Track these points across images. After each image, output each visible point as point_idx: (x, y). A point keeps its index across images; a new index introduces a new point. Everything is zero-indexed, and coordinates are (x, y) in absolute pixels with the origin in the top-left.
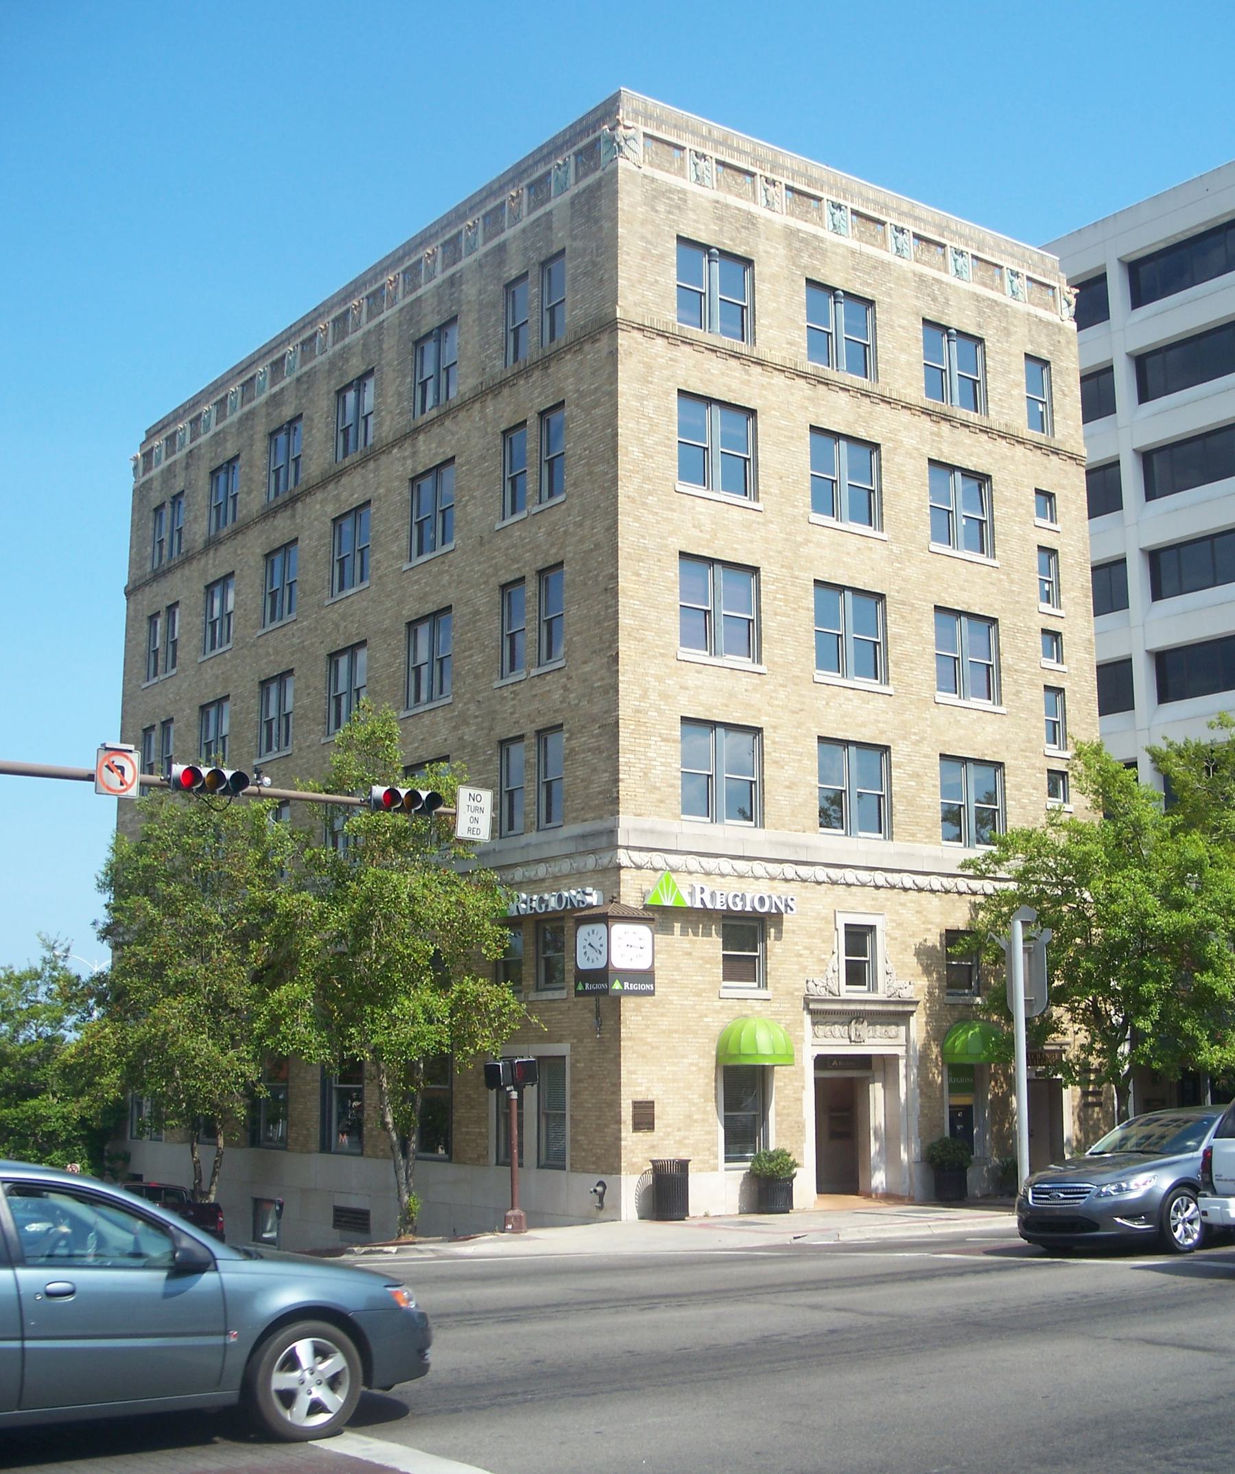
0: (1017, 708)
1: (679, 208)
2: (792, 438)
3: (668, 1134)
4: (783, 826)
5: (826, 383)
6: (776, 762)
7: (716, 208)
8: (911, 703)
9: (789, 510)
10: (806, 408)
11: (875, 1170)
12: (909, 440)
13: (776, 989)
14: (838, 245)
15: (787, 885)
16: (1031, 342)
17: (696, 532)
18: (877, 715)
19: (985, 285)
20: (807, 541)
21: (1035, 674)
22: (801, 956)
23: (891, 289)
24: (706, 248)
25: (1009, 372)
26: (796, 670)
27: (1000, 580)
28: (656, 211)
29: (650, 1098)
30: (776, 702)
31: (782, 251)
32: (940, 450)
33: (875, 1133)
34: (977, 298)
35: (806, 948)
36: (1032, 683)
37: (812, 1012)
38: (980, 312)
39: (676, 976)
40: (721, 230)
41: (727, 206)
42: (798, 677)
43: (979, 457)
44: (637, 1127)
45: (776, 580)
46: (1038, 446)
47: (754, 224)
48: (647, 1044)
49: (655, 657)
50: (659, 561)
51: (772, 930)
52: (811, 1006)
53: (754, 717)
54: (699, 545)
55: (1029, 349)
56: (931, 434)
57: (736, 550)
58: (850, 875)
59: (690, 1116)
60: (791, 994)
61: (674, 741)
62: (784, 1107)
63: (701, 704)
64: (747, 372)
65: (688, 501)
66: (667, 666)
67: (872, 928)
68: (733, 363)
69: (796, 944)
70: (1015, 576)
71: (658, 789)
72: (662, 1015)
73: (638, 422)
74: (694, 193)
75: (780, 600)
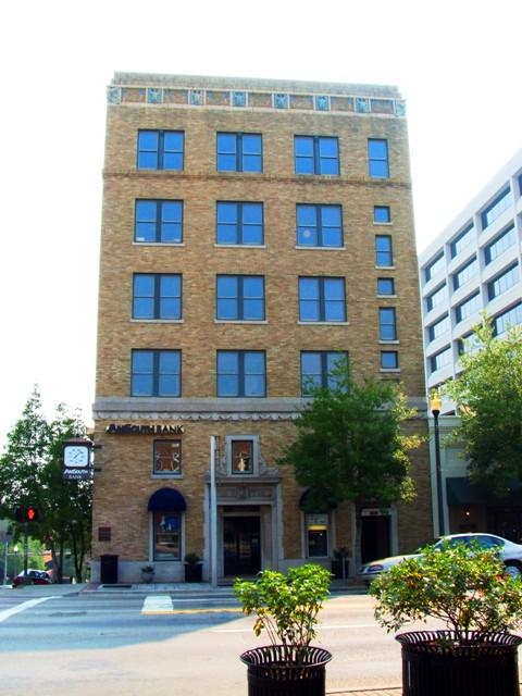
4: (193, 395)
5: (228, 179)
9: (201, 244)
16: (373, 131)
17: (143, 263)
20: (213, 257)
26: (203, 319)
38: (335, 124)
39: (125, 469)
44: (100, 539)
55: (371, 136)
58: (235, 417)
59: (132, 535)
63: (143, 341)
67: (252, 441)
70: (358, 253)
71: (116, 383)
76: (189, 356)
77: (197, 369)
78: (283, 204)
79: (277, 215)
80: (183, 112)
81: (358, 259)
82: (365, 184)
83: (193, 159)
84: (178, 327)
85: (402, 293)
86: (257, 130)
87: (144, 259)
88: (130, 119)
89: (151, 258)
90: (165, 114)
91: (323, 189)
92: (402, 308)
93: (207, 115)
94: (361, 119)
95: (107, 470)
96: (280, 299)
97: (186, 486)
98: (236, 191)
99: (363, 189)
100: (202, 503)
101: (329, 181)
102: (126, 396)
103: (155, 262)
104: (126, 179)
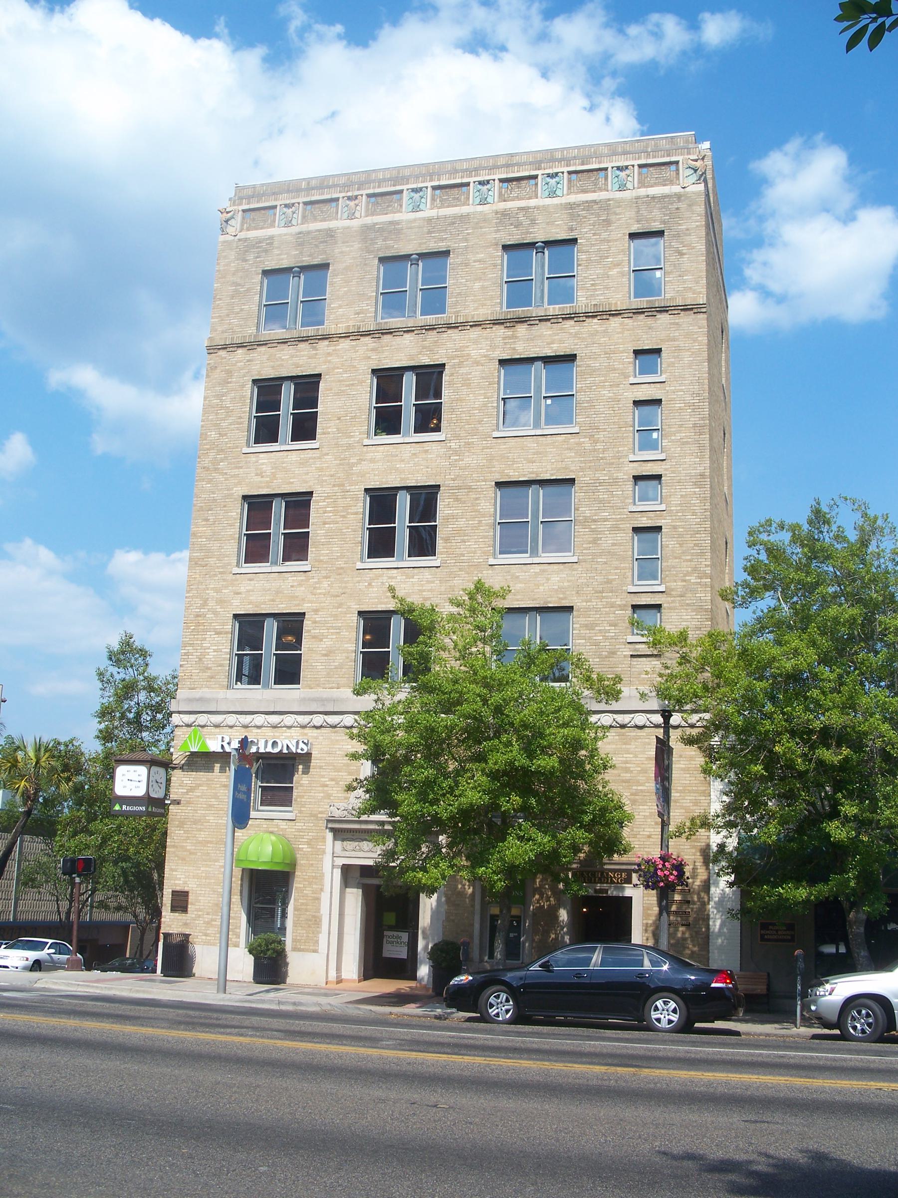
0: (593, 554)
1: (266, 251)
2: (353, 385)
3: (199, 916)
4: (318, 685)
6: (314, 637)
7: (299, 238)
8: (460, 570)
9: (345, 441)
10: (369, 358)
11: (421, 964)
12: (474, 353)
13: (301, 812)
14: (415, 220)
15: (319, 731)
16: (638, 221)
17: (258, 479)
18: (422, 585)
19: (584, 191)
20: (361, 460)
21: (622, 520)
22: (327, 786)
23: (468, 234)
24: (288, 270)
25: (607, 257)
26: (340, 563)
27: (579, 444)
28: (246, 261)
29: (186, 889)
30: (319, 591)
31: (357, 246)
32: (514, 349)
33: (423, 932)
34: (571, 206)
35: (332, 780)
36: (615, 528)
37: (332, 830)
38: (572, 217)
39: (213, 801)
40: (301, 253)
41: (309, 233)
42: (342, 568)
43: (561, 341)
44: (174, 909)
45: (328, 497)
46: (639, 312)
47: (332, 236)
48: (186, 850)
49: (215, 575)
50: (225, 506)
51: (301, 767)
52: (330, 825)
53: (298, 605)
54: (259, 487)
55: (635, 228)
56: (504, 338)
57: (292, 483)
60: (315, 816)
61: (226, 633)
62: (302, 904)
63: (250, 603)
64: (315, 349)
65: (253, 458)
66: (224, 580)
68: (302, 346)
69: (323, 776)
71: (209, 668)
72: (200, 830)
73: (217, 414)
74: (280, 235)
75: (330, 512)
76: (315, 622)
77: (327, 643)
78: (477, 363)
79: (467, 383)
80: (330, 234)
81: (599, 446)
82: (617, 314)
83: (340, 307)
84: (302, 577)
85: (676, 500)
86: (442, 246)
87: (260, 474)
88: (251, 257)
89: (267, 469)
90: (301, 240)
91: (545, 329)
92: (675, 527)
93: (366, 229)
94: (619, 202)
95: (189, 803)
96: (462, 523)
97: (299, 831)
98: (402, 352)
99: (615, 322)
100: (321, 860)
101: (556, 317)
102: (222, 687)
103: (274, 475)
104: (240, 351)
